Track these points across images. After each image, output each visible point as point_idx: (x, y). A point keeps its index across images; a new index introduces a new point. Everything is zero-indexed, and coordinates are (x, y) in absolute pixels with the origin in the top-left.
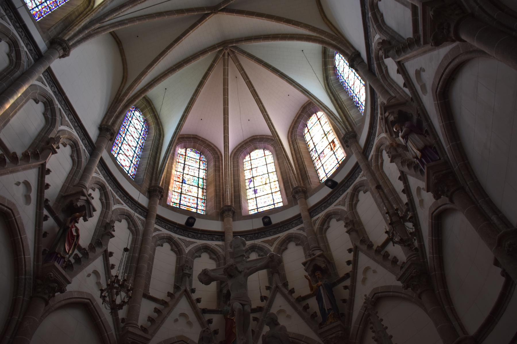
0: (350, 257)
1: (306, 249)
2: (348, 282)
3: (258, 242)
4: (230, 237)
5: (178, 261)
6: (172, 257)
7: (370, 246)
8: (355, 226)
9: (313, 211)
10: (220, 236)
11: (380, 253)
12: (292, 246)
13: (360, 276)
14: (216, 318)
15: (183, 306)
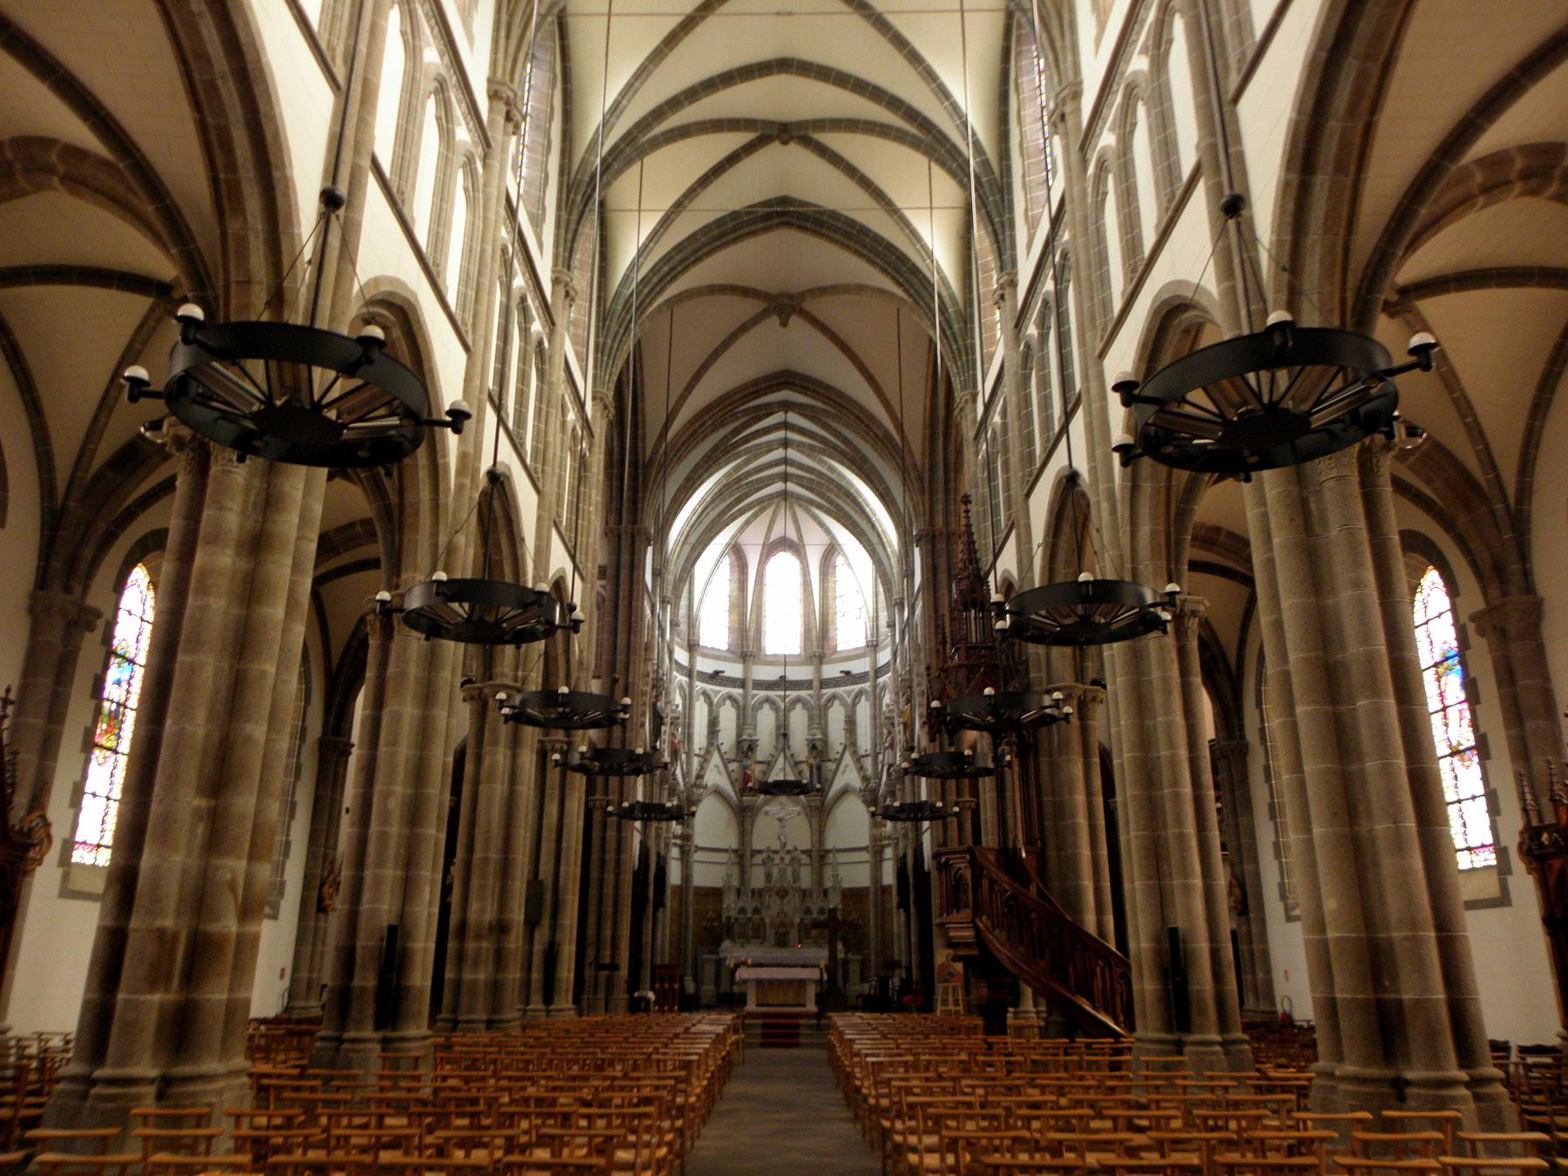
0: (840, 749)
1: (811, 718)
2: (832, 766)
3: (772, 694)
4: (750, 685)
5: (710, 712)
6: (705, 708)
7: (855, 752)
8: (851, 723)
9: (824, 683)
10: (742, 683)
11: (858, 760)
12: (799, 706)
13: (842, 768)
14: (734, 766)
15: (716, 759)
